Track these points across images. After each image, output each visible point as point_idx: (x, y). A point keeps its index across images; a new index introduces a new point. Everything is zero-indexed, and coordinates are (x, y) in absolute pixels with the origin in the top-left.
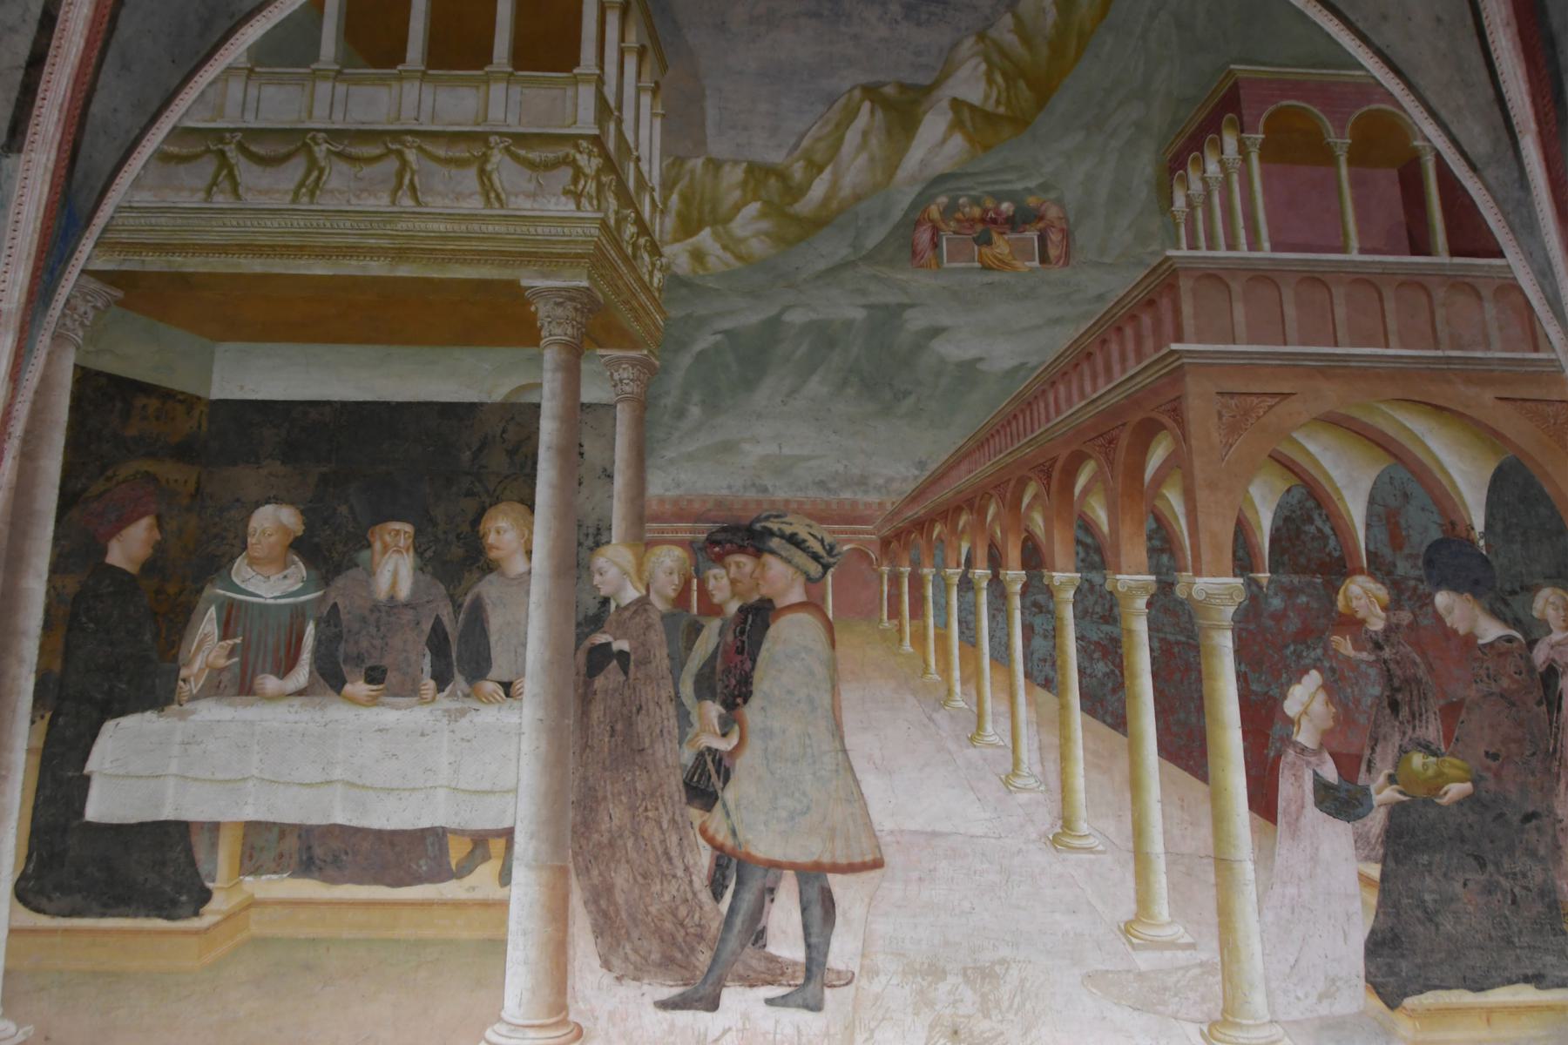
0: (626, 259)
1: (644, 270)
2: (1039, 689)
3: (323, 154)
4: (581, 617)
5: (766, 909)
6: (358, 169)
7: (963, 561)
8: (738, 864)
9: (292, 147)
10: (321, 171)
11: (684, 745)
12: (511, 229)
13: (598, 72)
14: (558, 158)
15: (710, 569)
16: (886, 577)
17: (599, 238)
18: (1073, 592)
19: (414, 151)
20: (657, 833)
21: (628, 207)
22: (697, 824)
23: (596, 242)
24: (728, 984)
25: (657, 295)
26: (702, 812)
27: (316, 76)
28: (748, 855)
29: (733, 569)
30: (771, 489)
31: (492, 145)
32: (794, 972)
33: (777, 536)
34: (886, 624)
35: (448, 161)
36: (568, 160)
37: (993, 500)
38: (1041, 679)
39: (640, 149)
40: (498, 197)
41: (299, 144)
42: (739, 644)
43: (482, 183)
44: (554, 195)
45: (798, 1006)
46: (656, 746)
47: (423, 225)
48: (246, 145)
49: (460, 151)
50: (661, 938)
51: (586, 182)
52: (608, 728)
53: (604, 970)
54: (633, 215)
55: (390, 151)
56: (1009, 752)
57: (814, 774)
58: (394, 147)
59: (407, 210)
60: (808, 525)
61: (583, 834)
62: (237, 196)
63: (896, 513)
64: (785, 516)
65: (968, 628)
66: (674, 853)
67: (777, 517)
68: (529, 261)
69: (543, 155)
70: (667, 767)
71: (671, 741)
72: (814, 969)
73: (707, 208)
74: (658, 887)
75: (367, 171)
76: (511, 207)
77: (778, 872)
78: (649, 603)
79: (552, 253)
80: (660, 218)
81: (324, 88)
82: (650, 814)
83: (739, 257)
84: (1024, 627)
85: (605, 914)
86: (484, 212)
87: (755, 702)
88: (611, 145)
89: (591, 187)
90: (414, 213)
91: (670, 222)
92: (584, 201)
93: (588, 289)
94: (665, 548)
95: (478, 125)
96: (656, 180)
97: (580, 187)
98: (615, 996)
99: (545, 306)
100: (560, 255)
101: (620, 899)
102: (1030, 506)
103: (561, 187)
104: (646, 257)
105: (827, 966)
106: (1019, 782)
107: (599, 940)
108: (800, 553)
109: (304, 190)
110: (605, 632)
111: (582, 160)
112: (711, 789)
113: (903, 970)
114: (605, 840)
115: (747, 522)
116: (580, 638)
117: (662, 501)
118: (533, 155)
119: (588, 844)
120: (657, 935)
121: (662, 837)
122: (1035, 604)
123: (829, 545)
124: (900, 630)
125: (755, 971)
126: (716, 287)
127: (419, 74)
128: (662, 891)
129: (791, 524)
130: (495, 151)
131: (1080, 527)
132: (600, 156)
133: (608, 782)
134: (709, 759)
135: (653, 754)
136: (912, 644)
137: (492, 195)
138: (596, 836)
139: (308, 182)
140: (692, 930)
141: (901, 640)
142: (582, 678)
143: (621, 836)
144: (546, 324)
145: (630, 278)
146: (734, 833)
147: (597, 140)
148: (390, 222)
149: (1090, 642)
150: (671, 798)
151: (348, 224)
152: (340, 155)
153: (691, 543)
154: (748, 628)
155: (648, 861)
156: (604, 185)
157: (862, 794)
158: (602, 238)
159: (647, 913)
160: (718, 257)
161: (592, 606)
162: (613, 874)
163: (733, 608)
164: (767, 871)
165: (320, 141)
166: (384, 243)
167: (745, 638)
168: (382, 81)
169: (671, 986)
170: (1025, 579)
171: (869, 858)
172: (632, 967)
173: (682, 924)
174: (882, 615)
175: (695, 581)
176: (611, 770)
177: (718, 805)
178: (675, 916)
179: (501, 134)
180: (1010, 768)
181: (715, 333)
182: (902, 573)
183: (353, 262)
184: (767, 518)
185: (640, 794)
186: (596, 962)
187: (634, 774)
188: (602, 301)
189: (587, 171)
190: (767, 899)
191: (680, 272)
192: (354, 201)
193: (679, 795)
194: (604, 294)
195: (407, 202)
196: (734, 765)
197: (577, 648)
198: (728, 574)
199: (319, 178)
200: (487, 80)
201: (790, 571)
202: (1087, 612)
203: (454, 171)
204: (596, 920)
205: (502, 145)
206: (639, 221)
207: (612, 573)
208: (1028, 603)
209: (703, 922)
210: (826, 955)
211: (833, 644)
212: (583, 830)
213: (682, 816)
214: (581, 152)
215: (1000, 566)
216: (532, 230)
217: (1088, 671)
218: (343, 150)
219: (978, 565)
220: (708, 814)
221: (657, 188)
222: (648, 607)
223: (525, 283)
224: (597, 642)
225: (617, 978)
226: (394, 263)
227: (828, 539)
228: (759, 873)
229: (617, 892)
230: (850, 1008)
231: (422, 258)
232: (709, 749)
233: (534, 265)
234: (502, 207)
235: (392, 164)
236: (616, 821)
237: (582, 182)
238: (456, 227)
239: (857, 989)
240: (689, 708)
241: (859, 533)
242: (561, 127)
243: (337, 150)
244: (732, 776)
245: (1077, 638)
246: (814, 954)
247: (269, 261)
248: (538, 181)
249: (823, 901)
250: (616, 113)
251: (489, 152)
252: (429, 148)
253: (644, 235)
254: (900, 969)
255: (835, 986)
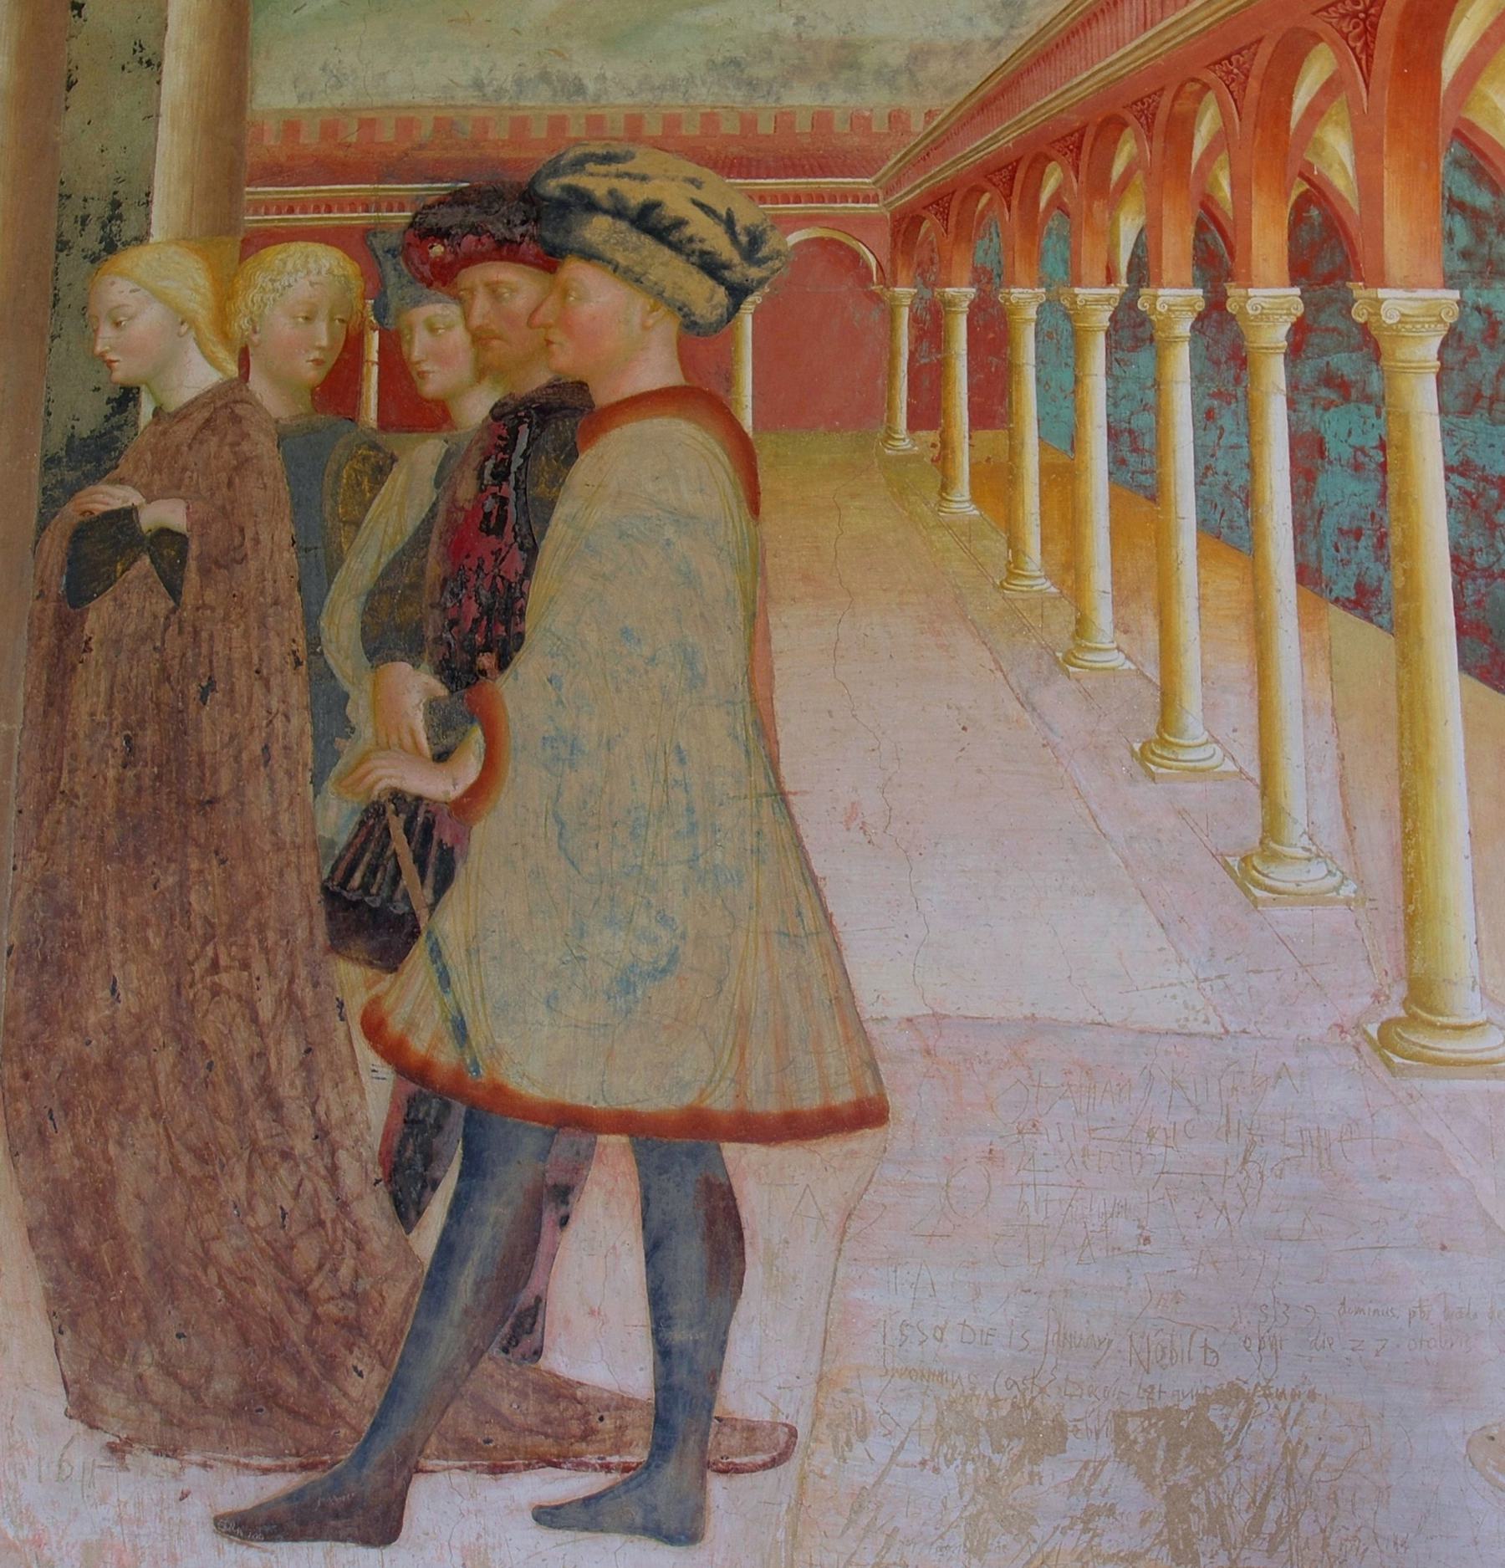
2: (1336, 613)
4: (57, 442)
5: (543, 1248)
7: (1123, 268)
8: (469, 1119)
11: (329, 786)
15: (417, 303)
16: (905, 314)
18: (1436, 343)
20: (243, 1034)
22: (355, 1007)
24: (429, 1464)
26: (371, 973)
28: (499, 1090)
29: (481, 305)
30: (591, 87)
32: (621, 1429)
33: (606, 212)
34: (904, 441)
37: (1210, 96)
38: (1344, 587)
42: (490, 505)
45: (631, 1529)
46: (250, 792)
50: (243, 1333)
52: (119, 742)
53: (78, 1427)
56: (1254, 792)
57: (692, 862)
60: (692, 181)
61: (34, 1037)
63: (937, 143)
64: (628, 157)
65: (1135, 450)
66: (289, 1088)
67: (608, 159)
70: (279, 847)
71: (291, 775)
72: (680, 1419)
74: (241, 1185)
77: (585, 1141)
78: (249, 401)
82: (225, 979)
84: (1295, 441)
85: (87, 1266)
87: (529, 666)
94: (297, 248)
98: (103, 1501)
101: (130, 1217)
102: (1315, 112)
105: (715, 1414)
106: (1283, 876)
107: (65, 1340)
108: (666, 253)
110: (121, 481)
112: (400, 909)
113: (939, 1422)
114: (95, 1055)
115: (525, 178)
116: (51, 503)
117: (291, 128)
119: (47, 1070)
120: (231, 1325)
121: (256, 1044)
122: (1329, 379)
123: (748, 232)
124: (943, 457)
125: (507, 1425)
128: (251, 1195)
129: (644, 178)
131: (1457, 163)
133: (112, 891)
134: (397, 825)
135: (240, 813)
136: (976, 498)
138: (69, 1043)
140: (332, 1309)
141: (945, 487)
142: (51, 607)
143: (141, 1044)
146: (461, 1031)
149: (1485, 479)
150: (284, 934)
153: (367, 232)
154: (517, 461)
155: (215, 1112)
157: (828, 917)
159: (207, 1260)
161: (90, 415)
162: (113, 1149)
163: (476, 408)
164: (552, 1135)
167: (508, 489)
169: (266, 1471)
170: (1299, 309)
171: (843, 1097)
172: (156, 1417)
173: (303, 1293)
174: (891, 419)
175: (374, 341)
176: (122, 860)
177: (419, 953)
178: (285, 1268)
180: (1251, 832)
182: (950, 303)
184: (579, 164)
185: (198, 924)
186: (56, 1404)
187: (185, 869)
190: (549, 1216)
193: (309, 925)
196: (463, 837)
197: (42, 527)
198: (466, 316)
201: (637, 305)
202: (1479, 396)
204: (58, 1280)
207: (148, 320)
208: (1308, 371)
209: (364, 1285)
210: (713, 1379)
211: (755, 508)
212: (34, 1025)
213: (316, 985)
215: (1230, 276)
217: (1481, 560)
219: (1167, 276)
220: (389, 977)
222: (240, 410)
224: (100, 508)
225: (112, 1449)
227: (747, 216)
228: (530, 1140)
229: (124, 1200)
230: (781, 1535)
232: (397, 796)
236: (129, 1001)
239: (803, 1479)
240: (347, 686)
241: (833, 199)
244: (460, 870)
245: (1449, 469)
246: (681, 1375)
249: (711, 1222)
254: (930, 1417)
255: (738, 1470)
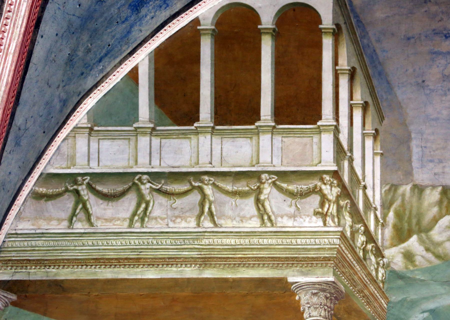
0: (359, 260)
1: (372, 268)
3: (148, 191)
6: (172, 201)
9: (126, 186)
10: (147, 203)
12: (280, 241)
13: (335, 123)
14: (310, 188)
17: (339, 245)
19: (210, 187)
21: (359, 222)
23: (338, 248)
25: (381, 285)
27: (137, 132)
31: (263, 181)
35: (234, 194)
36: (316, 190)
39: (366, 180)
40: (269, 218)
41: (130, 184)
43: (259, 209)
44: (308, 216)
47: (219, 241)
48: (94, 186)
49: (242, 186)
51: (329, 206)
54: (362, 228)
55: (194, 188)
58: (196, 184)
59: (209, 230)
62: (92, 225)
68: (293, 264)
69: (299, 187)
73: (414, 221)
75: (179, 202)
76: (278, 225)
79: (308, 258)
80: (382, 230)
81: (144, 141)
83: (438, 257)
86: (260, 230)
88: (346, 178)
89: (333, 209)
90: (213, 232)
91: (389, 232)
92: (328, 219)
93: (334, 282)
95: (254, 166)
96: (377, 202)
97: (326, 210)
99: (305, 296)
100: (313, 259)
103: (312, 210)
104: (373, 258)
109: (136, 218)
111: (326, 189)
118: (292, 187)
126: (423, 278)
127: (210, 129)
130: (266, 185)
132: (338, 186)
137: (266, 217)
139: (139, 212)
144: (307, 308)
145: (362, 274)
147: (336, 174)
148: (197, 239)
151: (168, 242)
152: (159, 191)
156: (342, 207)
158: (342, 245)
160: (423, 257)
165: (145, 181)
166: (194, 254)
168: (184, 135)
179: (270, 173)
181: (423, 312)
183: (174, 269)
188: (344, 291)
189: (330, 197)
191: (396, 268)
192: (171, 224)
194: (345, 286)
195: (207, 224)
199: (146, 209)
200: (258, 132)
203: (239, 200)
205: (270, 181)
206: (367, 232)
214: (325, 184)
216: (294, 241)
218: (161, 187)
221: (379, 207)
223: (290, 280)
226: (201, 268)
231: (220, 264)
233: (297, 267)
234: (272, 226)
235: (195, 197)
237: (327, 206)
238: (242, 241)
242: (312, 165)
243: (158, 188)
247: (116, 270)
248: (296, 206)
250: (349, 154)
251: (262, 186)
252: (221, 184)
253: (370, 243)
